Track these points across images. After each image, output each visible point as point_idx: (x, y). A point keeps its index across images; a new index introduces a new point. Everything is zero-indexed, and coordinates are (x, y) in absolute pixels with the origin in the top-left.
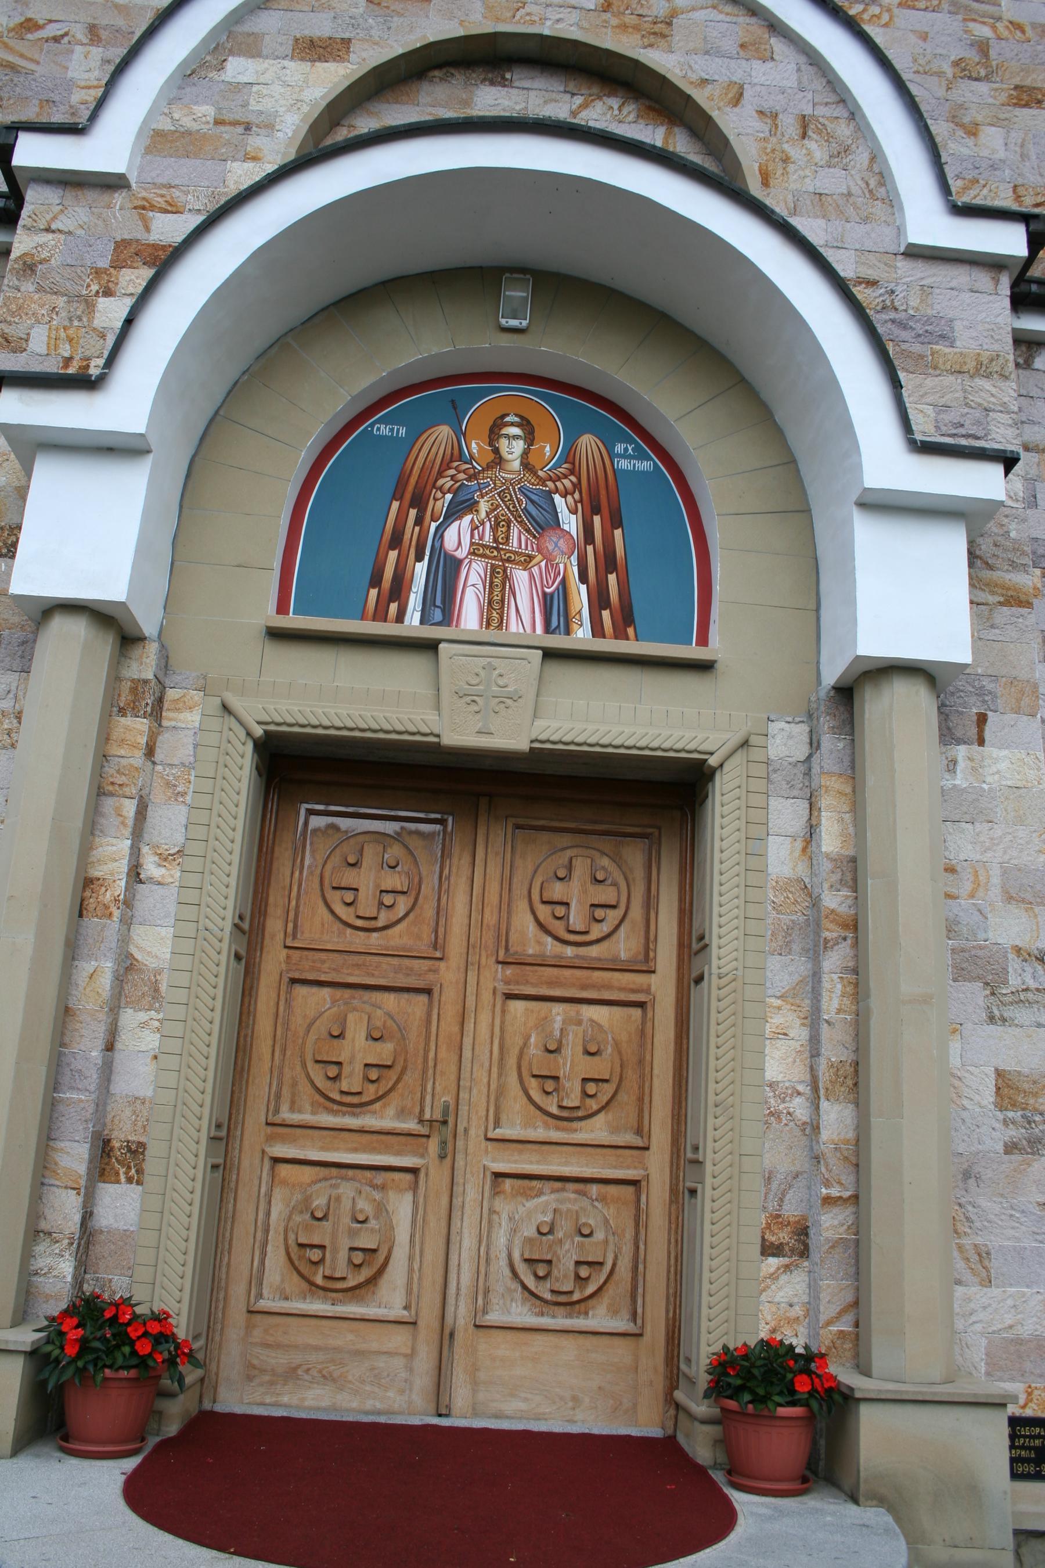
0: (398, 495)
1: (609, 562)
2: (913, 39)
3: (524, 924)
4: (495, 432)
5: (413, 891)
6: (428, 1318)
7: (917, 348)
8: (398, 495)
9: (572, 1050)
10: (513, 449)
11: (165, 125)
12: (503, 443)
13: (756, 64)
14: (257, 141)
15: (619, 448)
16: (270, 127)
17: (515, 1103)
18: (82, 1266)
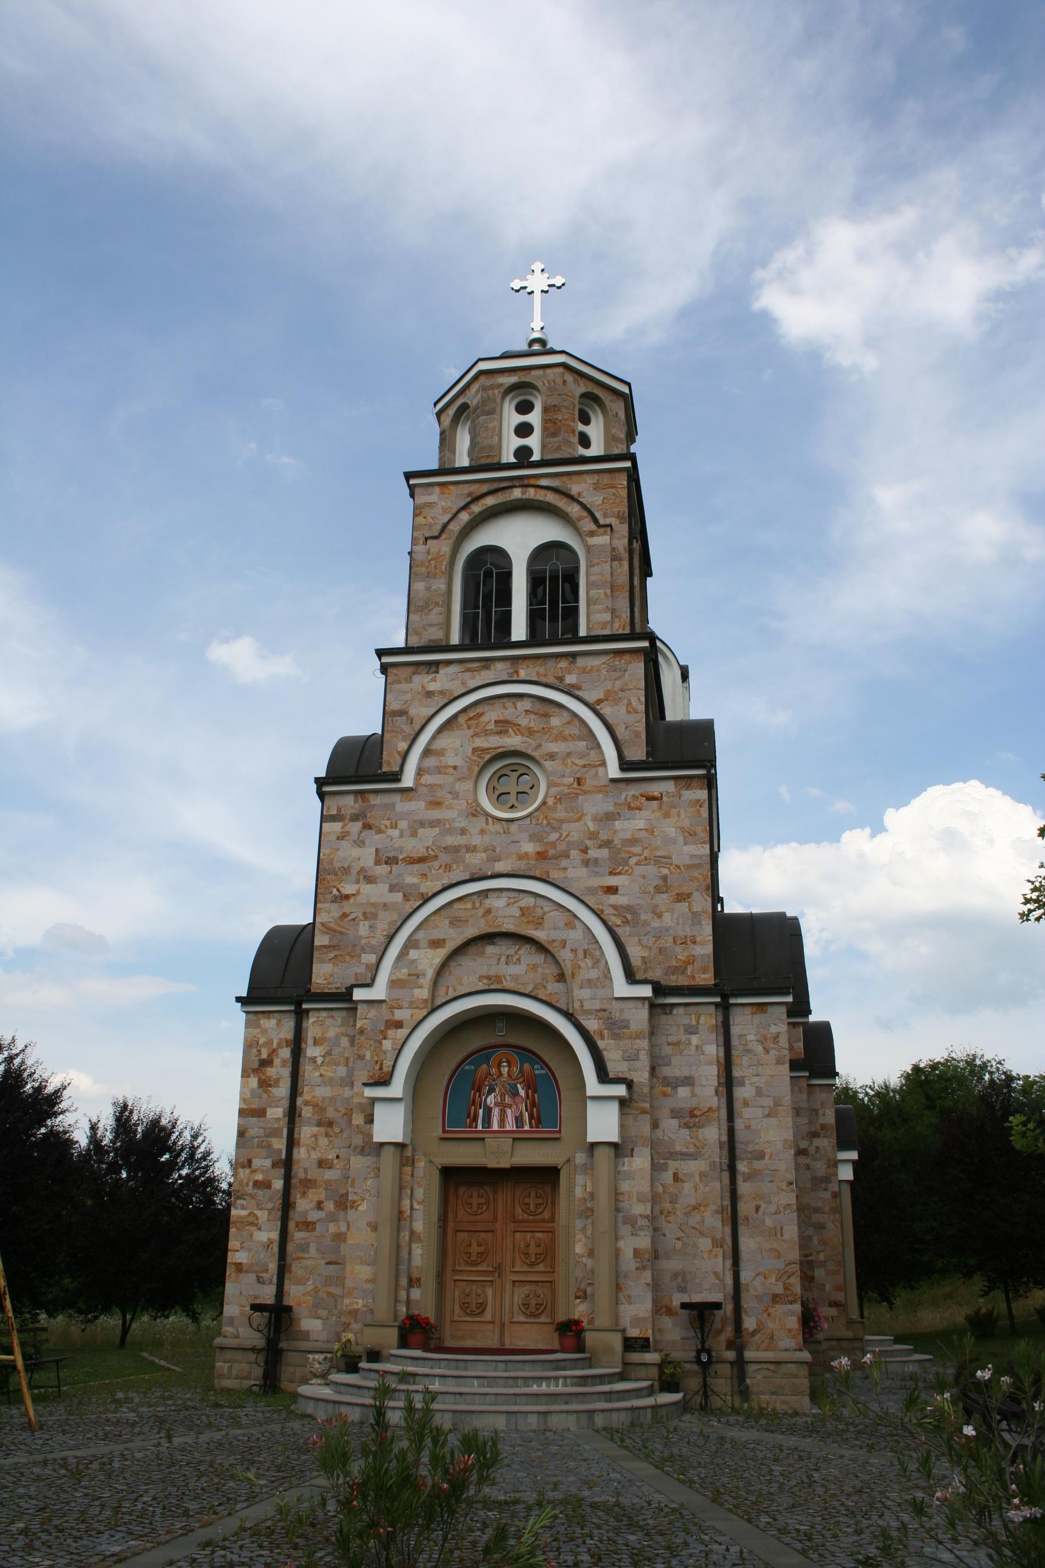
0: (473, 1088)
1: (534, 1104)
2: (640, 879)
3: (519, 1210)
4: (499, 1066)
5: (487, 1203)
6: (497, 1321)
7: (617, 1031)
8: (473, 1088)
9: (532, 1245)
11: (394, 978)
12: (502, 1069)
13: (570, 931)
14: (421, 981)
15: (536, 1067)
16: (424, 975)
17: (518, 1262)
18: (408, 1309)
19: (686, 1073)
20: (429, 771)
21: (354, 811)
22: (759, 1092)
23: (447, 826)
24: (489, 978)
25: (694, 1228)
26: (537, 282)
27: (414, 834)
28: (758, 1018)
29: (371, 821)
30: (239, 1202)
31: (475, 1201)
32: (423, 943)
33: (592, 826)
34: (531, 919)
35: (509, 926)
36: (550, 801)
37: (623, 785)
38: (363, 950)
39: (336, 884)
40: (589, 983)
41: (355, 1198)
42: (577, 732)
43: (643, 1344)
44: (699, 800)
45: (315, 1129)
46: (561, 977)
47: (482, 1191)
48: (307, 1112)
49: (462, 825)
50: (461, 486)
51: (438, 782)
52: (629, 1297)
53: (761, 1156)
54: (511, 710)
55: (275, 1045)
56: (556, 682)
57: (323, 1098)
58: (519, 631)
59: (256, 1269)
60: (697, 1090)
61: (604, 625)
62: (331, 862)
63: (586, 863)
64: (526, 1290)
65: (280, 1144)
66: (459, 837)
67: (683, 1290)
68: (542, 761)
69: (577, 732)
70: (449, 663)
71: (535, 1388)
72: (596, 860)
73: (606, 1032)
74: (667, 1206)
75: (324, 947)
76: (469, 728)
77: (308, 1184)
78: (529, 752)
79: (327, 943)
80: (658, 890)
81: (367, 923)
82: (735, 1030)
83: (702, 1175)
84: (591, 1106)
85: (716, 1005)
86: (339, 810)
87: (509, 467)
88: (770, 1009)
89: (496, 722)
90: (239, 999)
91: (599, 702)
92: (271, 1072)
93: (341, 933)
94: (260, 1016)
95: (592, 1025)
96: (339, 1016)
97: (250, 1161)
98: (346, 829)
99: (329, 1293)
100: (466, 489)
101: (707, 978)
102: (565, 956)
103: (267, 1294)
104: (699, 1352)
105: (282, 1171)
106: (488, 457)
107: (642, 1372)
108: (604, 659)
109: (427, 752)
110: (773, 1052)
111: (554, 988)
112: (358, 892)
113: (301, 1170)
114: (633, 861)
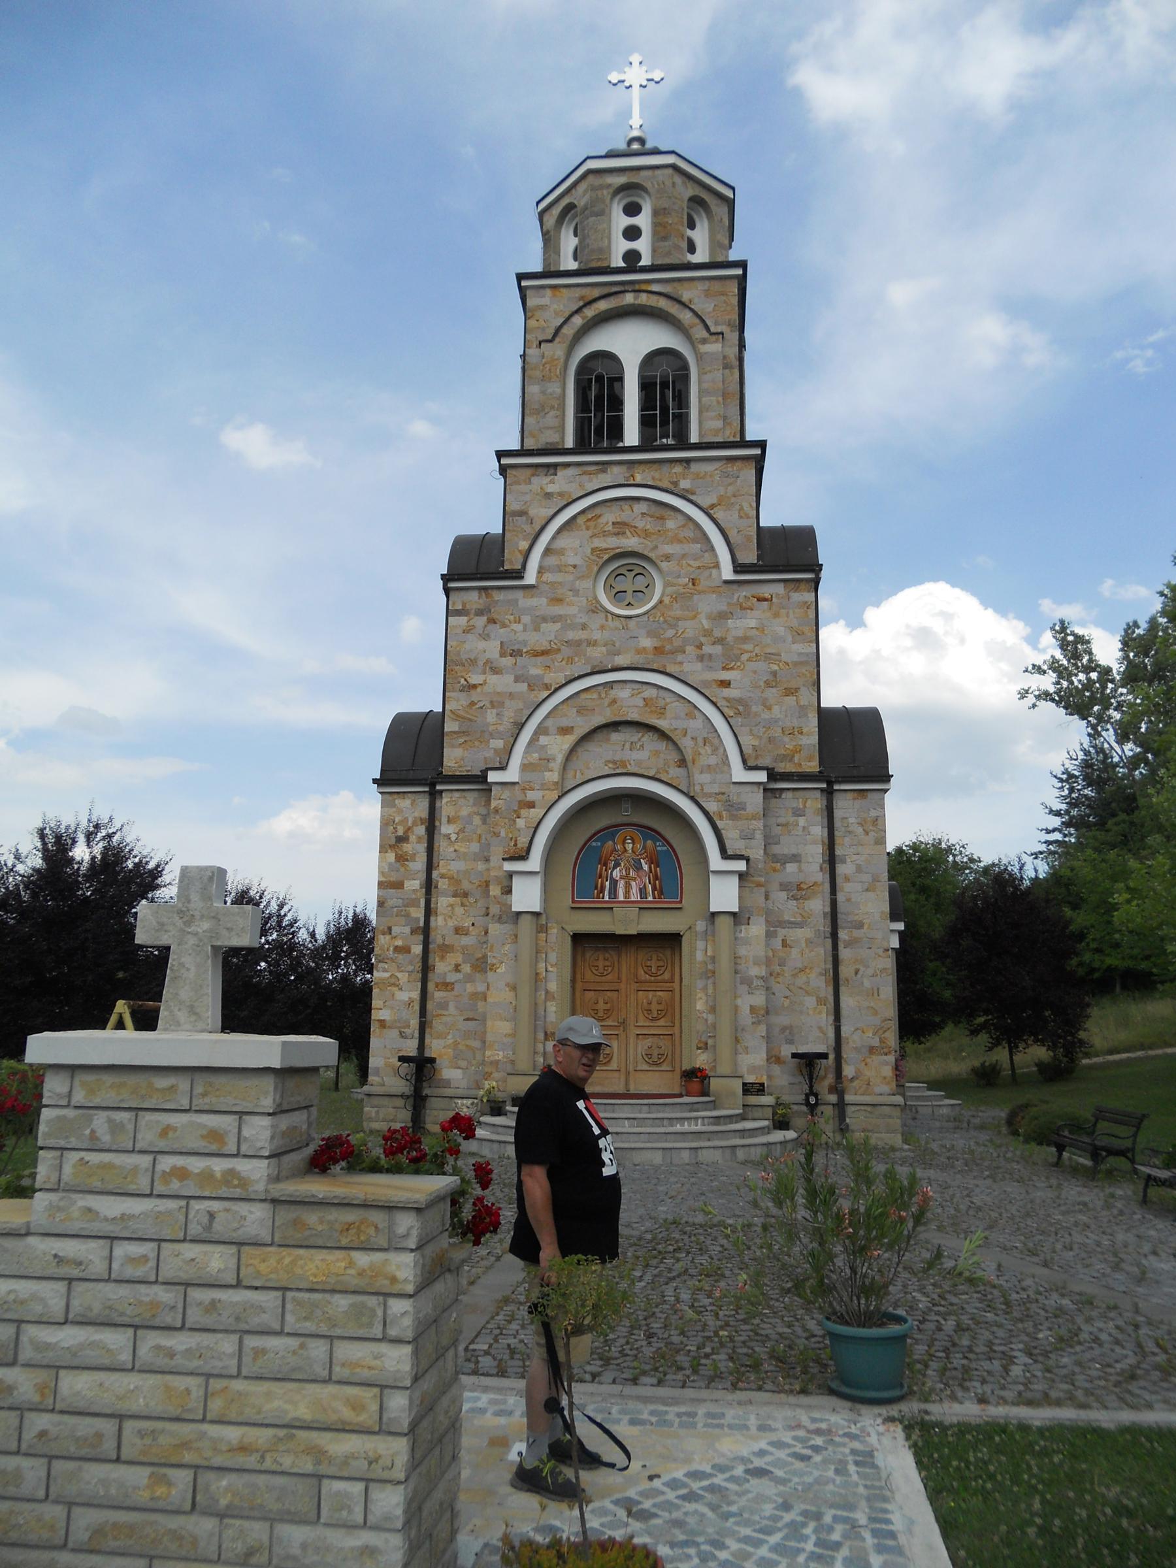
1: (656, 878)
4: (624, 843)
6: (623, 1070)
7: (735, 813)
10: (629, 847)
11: (526, 762)
14: (551, 765)
16: (554, 759)
17: (641, 1016)
19: (794, 851)
20: (549, 569)
21: (479, 607)
22: (859, 869)
23: (569, 621)
24: (614, 762)
25: (801, 988)
26: (635, 75)
27: (537, 629)
28: (859, 803)
29: (495, 616)
30: (381, 965)
31: (601, 964)
32: (552, 730)
33: (706, 624)
34: (654, 709)
35: (633, 716)
36: (667, 600)
37: (735, 587)
38: (492, 736)
39: (464, 674)
40: (709, 768)
41: (494, 961)
42: (692, 535)
43: (760, 1089)
44: (806, 602)
45: (451, 900)
46: (682, 763)
47: (607, 955)
48: (443, 884)
49: (583, 620)
50: (573, 289)
51: (560, 580)
52: (747, 1048)
53: (860, 925)
54: (628, 512)
55: (410, 824)
56: (671, 487)
57: (458, 871)
58: (632, 434)
59: (399, 1025)
60: (803, 866)
61: (717, 432)
62: (458, 653)
63: (701, 658)
64: (648, 1042)
65: (418, 913)
66: (581, 632)
67: (790, 1042)
68: (658, 562)
69: (692, 535)
70: (567, 465)
71: (678, 1128)
72: (710, 655)
73: (724, 813)
74: (777, 969)
75: (454, 732)
76: (588, 528)
77: (446, 949)
78: (646, 553)
79: (456, 729)
80: (768, 684)
81: (494, 711)
82: (838, 814)
83: (809, 942)
84: (712, 878)
85: (822, 790)
86: (464, 604)
87: (618, 271)
88: (870, 795)
89: (613, 523)
90: (375, 781)
91: (713, 506)
92: (407, 847)
93: (470, 720)
94: (395, 796)
95: (712, 807)
96: (471, 797)
97: (390, 929)
98: (471, 623)
99: (467, 1046)
100: (578, 292)
101: (813, 766)
102: (686, 743)
103: (410, 1048)
104: (807, 1096)
105: (421, 937)
106: (599, 259)
107: (758, 1113)
108: (717, 465)
109: (548, 551)
110: (872, 834)
111: (675, 773)
112: (485, 682)
113: (439, 937)
114: (745, 657)
